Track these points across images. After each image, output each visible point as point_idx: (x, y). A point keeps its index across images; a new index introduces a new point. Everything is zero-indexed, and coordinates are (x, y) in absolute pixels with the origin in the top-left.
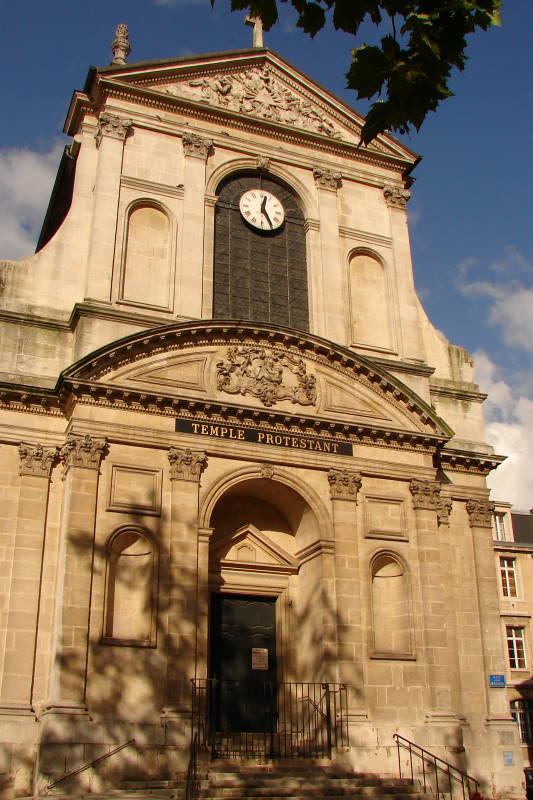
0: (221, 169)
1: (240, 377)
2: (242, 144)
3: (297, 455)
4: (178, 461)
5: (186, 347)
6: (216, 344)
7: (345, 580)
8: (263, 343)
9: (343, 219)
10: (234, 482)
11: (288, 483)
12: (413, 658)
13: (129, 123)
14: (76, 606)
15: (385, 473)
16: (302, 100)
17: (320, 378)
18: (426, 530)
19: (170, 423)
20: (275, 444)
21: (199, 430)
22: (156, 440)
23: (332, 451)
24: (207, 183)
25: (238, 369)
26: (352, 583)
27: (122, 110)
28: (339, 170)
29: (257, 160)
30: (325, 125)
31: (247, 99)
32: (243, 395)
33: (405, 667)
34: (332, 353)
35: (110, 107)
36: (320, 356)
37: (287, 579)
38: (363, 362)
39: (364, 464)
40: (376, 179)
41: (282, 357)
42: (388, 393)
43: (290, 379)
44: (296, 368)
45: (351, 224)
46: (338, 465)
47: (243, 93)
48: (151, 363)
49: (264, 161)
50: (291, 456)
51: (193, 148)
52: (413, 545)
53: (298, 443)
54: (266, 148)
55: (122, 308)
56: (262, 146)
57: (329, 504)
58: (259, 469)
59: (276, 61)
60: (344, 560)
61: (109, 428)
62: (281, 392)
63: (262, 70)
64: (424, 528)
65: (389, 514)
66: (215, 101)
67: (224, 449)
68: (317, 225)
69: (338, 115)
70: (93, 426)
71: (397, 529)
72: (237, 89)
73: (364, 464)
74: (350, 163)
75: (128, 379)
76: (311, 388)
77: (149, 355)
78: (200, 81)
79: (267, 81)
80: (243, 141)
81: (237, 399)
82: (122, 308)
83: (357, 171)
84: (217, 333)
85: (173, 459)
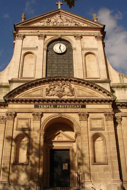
0: (48, 41)
1: (52, 91)
2: (53, 33)
3: (69, 110)
4: (35, 115)
5: (37, 86)
6: (46, 84)
7: (84, 143)
8: (59, 82)
10: (51, 119)
11: (67, 118)
12: (107, 163)
13: (23, 35)
14: (7, 155)
15: (96, 111)
16: (71, 19)
17: (76, 89)
18: (110, 126)
20: (62, 108)
21: (41, 107)
22: (29, 111)
25: (52, 90)
26: (85, 143)
27: (22, 32)
28: (81, 34)
30: (77, 23)
31: (55, 22)
32: (53, 96)
33: (104, 166)
34: (78, 81)
36: (75, 82)
37: (72, 144)
38: (88, 82)
39: (89, 110)
40: (92, 34)
41: (64, 84)
42: (96, 89)
43: (67, 90)
44: (68, 87)
45: (85, 47)
46: (81, 111)
47: (54, 21)
48: (28, 92)
49: (59, 36)
50: (67, 110)
51: (40, 37)
52: (106, 131)
53: (69, 106)
54: (59, 33)
55: (21, 79)
57: (79, 122)
59: (62, 11)
60: (83, 137)
61: (16, 109)
62: (64, 94)
63: (59, 14)
64: (109, 125)
65: (98, 123)
66: (46, 25)
67: (47, 111)
68: (75, 49)
69: (81, 20)
70: (12, 109)
71: (101, 127)
72: (53, 20)
73: (89, 110)
74: (85, 31)
75: (22, 96)
76: (73, 91)
77: (27, 90)
78: (42, 21)
80: (54, 32)
81: (52, 97)
82: (21, 79)
83: (87, 33)
85: (33, 115)
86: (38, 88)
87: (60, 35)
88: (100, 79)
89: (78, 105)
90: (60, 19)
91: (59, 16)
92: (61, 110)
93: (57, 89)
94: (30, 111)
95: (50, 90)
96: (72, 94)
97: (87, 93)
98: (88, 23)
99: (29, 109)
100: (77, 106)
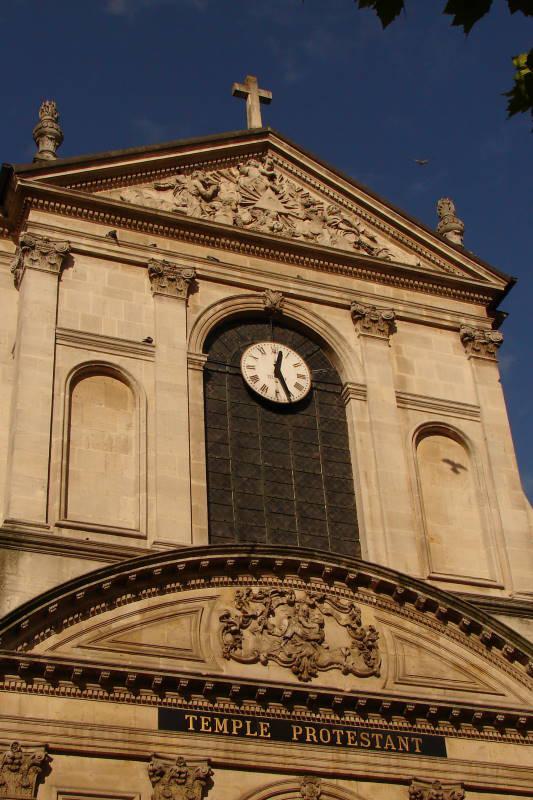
0: (211, 312)
2: (239, 274)
4: (166, 778)
5: (169, 591)
6: (217, 584)
8: (292, 579)
9: (402, 381)
13: (66, 247)
15: (503, 783)
16: (326, 204)
17: (384, 631)
19: (149, 716)
20: (320, 743)
21: (197, 724)
22: (127, 745)
23: (412, 750)
24: (189, 337)
25: (254, 624)
29: (264, 297)
30: (364, 239)
31: (243, 205)
32: (265, 664)
34: (400, 591)
35: (36, 225)
36: (382, 595)
38: (453, 604)
40: (448, 317)
41: (322, 600)
42: (495, 650)
43: (337, 636)
44: (344, 617)
45: (415, 388)
46: (424, 773)
47: (237, 197)
48: (115, 620)
49: (274, 297)
51: (165, 283)
53: (357, 739)
54: (277, 278)
55: (66, 533)
56: (270, 275)
58: (297, 785)
59: (284, 147)
61: (50, 729)
62: (325, 658)
63: (263, 162)
66: (194, 210)
67: (238, 756)
68: (362, 392)
72: (228, 191)
73: (467, 769)
74: (406, 295)
75: (79, 646)
76: (371, 648)
77: (112, 607)
78: (171, 181)
79: (272, 178)
80: (242, 269)
82: (66, 533)
83: (418, 306)
84: (218, 567)
85: (156, 775)
86: (172, 604)
87: (274, 289)
88: (504, 594)
89: (403, 735)
90: (269, 190)
91: (263, 174)
92: (318, 755)
93: (281, 623)
94: (133, 746)
95: (245, 628)
96: (366, 667)
97: (444, 668)
98: (420, 247)
99: (127, 737)
100: (400, 738)
